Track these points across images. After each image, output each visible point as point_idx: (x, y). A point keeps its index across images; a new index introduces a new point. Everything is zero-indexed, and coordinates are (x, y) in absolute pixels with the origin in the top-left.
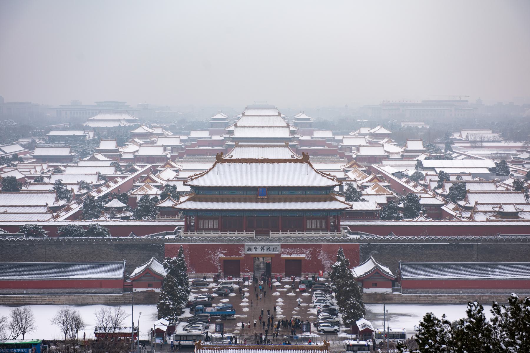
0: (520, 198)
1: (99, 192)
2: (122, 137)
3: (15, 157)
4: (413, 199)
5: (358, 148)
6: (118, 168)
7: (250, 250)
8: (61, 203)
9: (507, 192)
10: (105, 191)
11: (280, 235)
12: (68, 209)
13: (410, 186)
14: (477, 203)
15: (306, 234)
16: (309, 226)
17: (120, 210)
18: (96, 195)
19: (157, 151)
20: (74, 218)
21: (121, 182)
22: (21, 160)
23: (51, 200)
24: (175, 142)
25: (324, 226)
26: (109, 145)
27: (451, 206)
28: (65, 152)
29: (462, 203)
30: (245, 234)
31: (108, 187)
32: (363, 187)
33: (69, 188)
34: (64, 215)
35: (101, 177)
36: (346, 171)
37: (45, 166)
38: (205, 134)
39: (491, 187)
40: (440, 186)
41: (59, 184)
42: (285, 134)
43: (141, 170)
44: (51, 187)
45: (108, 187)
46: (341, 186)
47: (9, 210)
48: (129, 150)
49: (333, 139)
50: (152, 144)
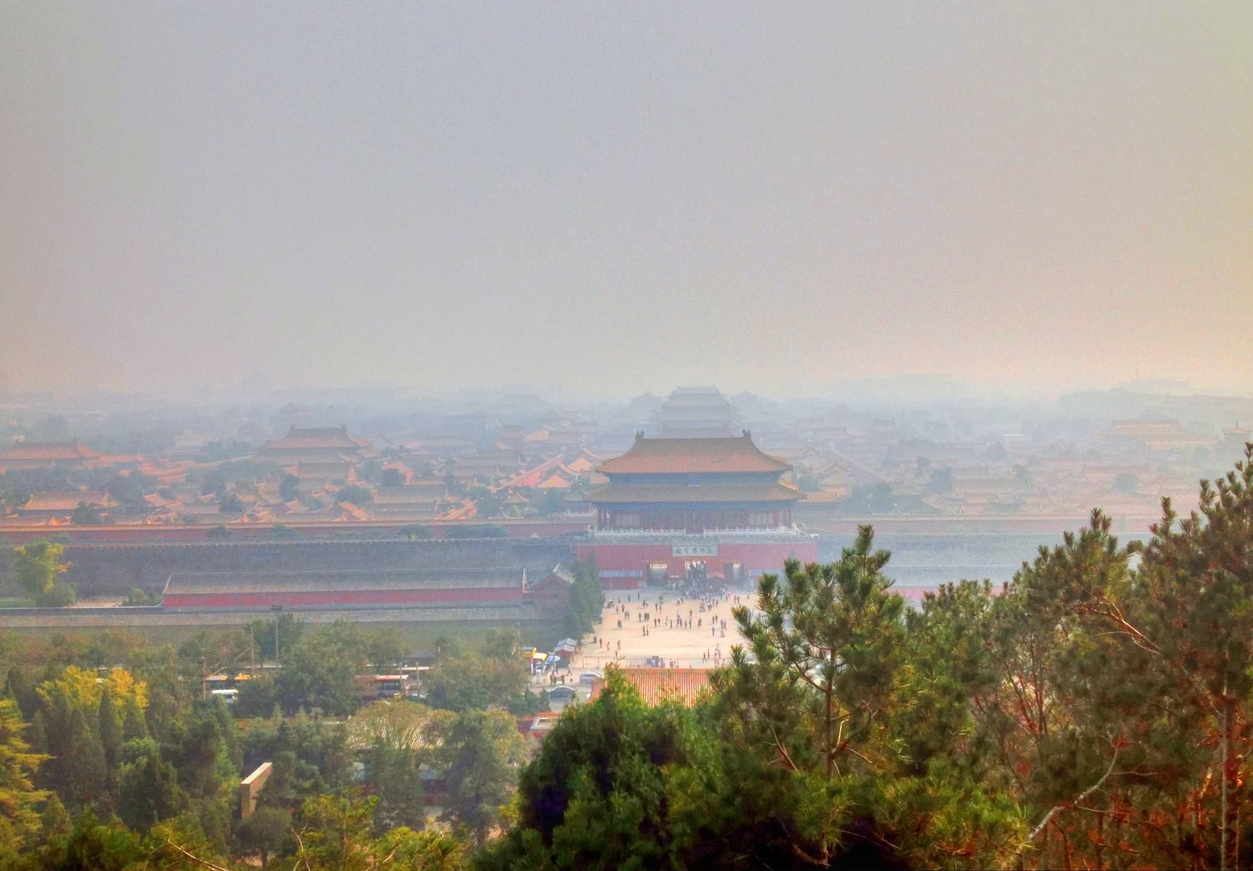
1: (498, 485)
7: (678, 552)
10: (505, 483)
11: (717, 532)
12: (459, 506)
15: (748, 532)
16: (752, 522)
17: (522, 505)
25: (771, 522)
30: (672, 532)
31: (509, 479)
45: (509, 479)
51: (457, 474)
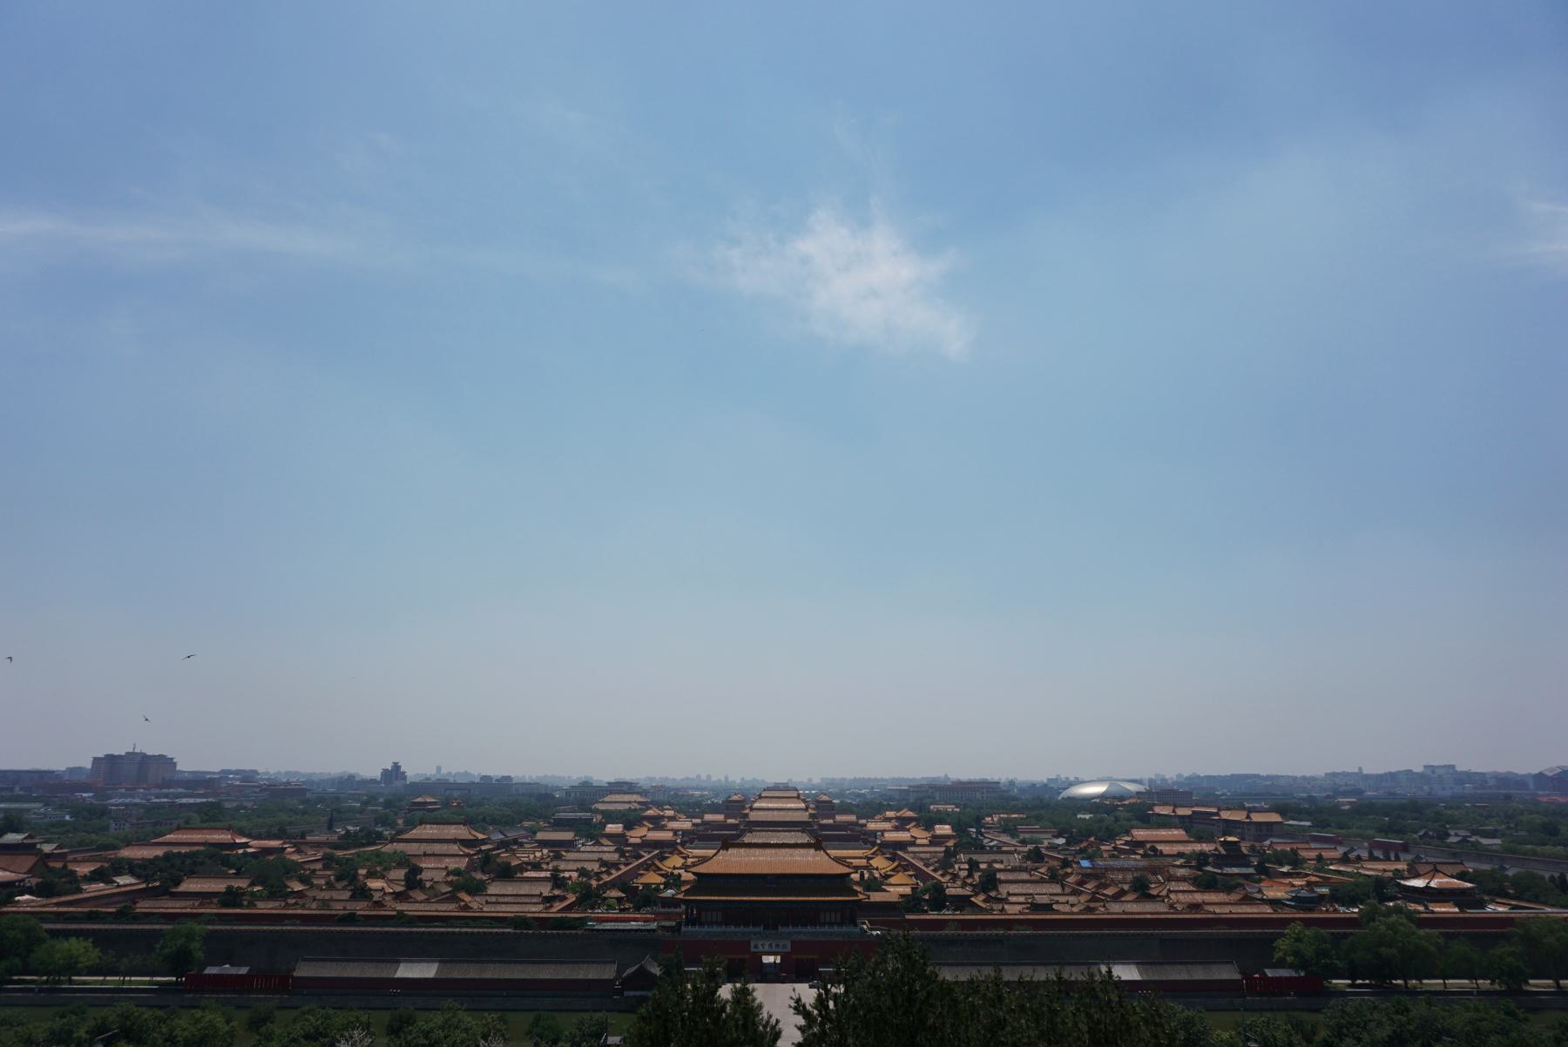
0: (1057, 889)
1: (599, 879)
2: (631, 820)
3: (515, 842)
4: (938, 889)
5: (883, 831)
6: (622, 854)
8: (557, 892)
9: (1041, 881)
10: (606, 878)
12: (564, 898)
13: (937, 875)
14: (1009, 894)
17: (619, 900)
18: (594, 883)
19: (666, 836)
20: (569, 908)
21: (624, 869)
22: (521, 845)
23: (546, 890)
24: (687, 825)
26: (613, 828)
27: (982, 897)
28: (568, 836)
29: (993, 894)
32: (887, 877)
33: (567, 875)
34: (558, 906)
35: (603, 863)
36: (869, 859)
37: (545, 851)
38: (720, 817)
39: (1025, 876)
40: (970, 875)
41: (556, 870)
42: (804, 817)
43: (647, 856)
44: (548, 874)
46: (862, 875)
47: (501, 899)
48: (635, 835)
49: (857, 824)
50: (663, 828)
51: (562, 866)
